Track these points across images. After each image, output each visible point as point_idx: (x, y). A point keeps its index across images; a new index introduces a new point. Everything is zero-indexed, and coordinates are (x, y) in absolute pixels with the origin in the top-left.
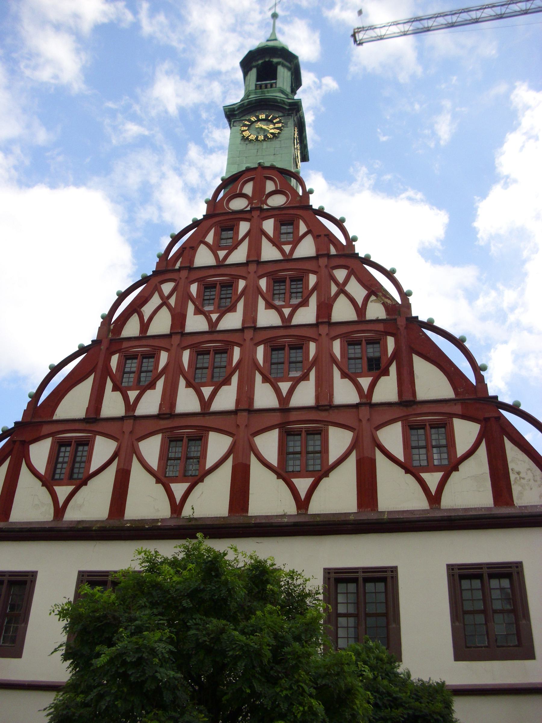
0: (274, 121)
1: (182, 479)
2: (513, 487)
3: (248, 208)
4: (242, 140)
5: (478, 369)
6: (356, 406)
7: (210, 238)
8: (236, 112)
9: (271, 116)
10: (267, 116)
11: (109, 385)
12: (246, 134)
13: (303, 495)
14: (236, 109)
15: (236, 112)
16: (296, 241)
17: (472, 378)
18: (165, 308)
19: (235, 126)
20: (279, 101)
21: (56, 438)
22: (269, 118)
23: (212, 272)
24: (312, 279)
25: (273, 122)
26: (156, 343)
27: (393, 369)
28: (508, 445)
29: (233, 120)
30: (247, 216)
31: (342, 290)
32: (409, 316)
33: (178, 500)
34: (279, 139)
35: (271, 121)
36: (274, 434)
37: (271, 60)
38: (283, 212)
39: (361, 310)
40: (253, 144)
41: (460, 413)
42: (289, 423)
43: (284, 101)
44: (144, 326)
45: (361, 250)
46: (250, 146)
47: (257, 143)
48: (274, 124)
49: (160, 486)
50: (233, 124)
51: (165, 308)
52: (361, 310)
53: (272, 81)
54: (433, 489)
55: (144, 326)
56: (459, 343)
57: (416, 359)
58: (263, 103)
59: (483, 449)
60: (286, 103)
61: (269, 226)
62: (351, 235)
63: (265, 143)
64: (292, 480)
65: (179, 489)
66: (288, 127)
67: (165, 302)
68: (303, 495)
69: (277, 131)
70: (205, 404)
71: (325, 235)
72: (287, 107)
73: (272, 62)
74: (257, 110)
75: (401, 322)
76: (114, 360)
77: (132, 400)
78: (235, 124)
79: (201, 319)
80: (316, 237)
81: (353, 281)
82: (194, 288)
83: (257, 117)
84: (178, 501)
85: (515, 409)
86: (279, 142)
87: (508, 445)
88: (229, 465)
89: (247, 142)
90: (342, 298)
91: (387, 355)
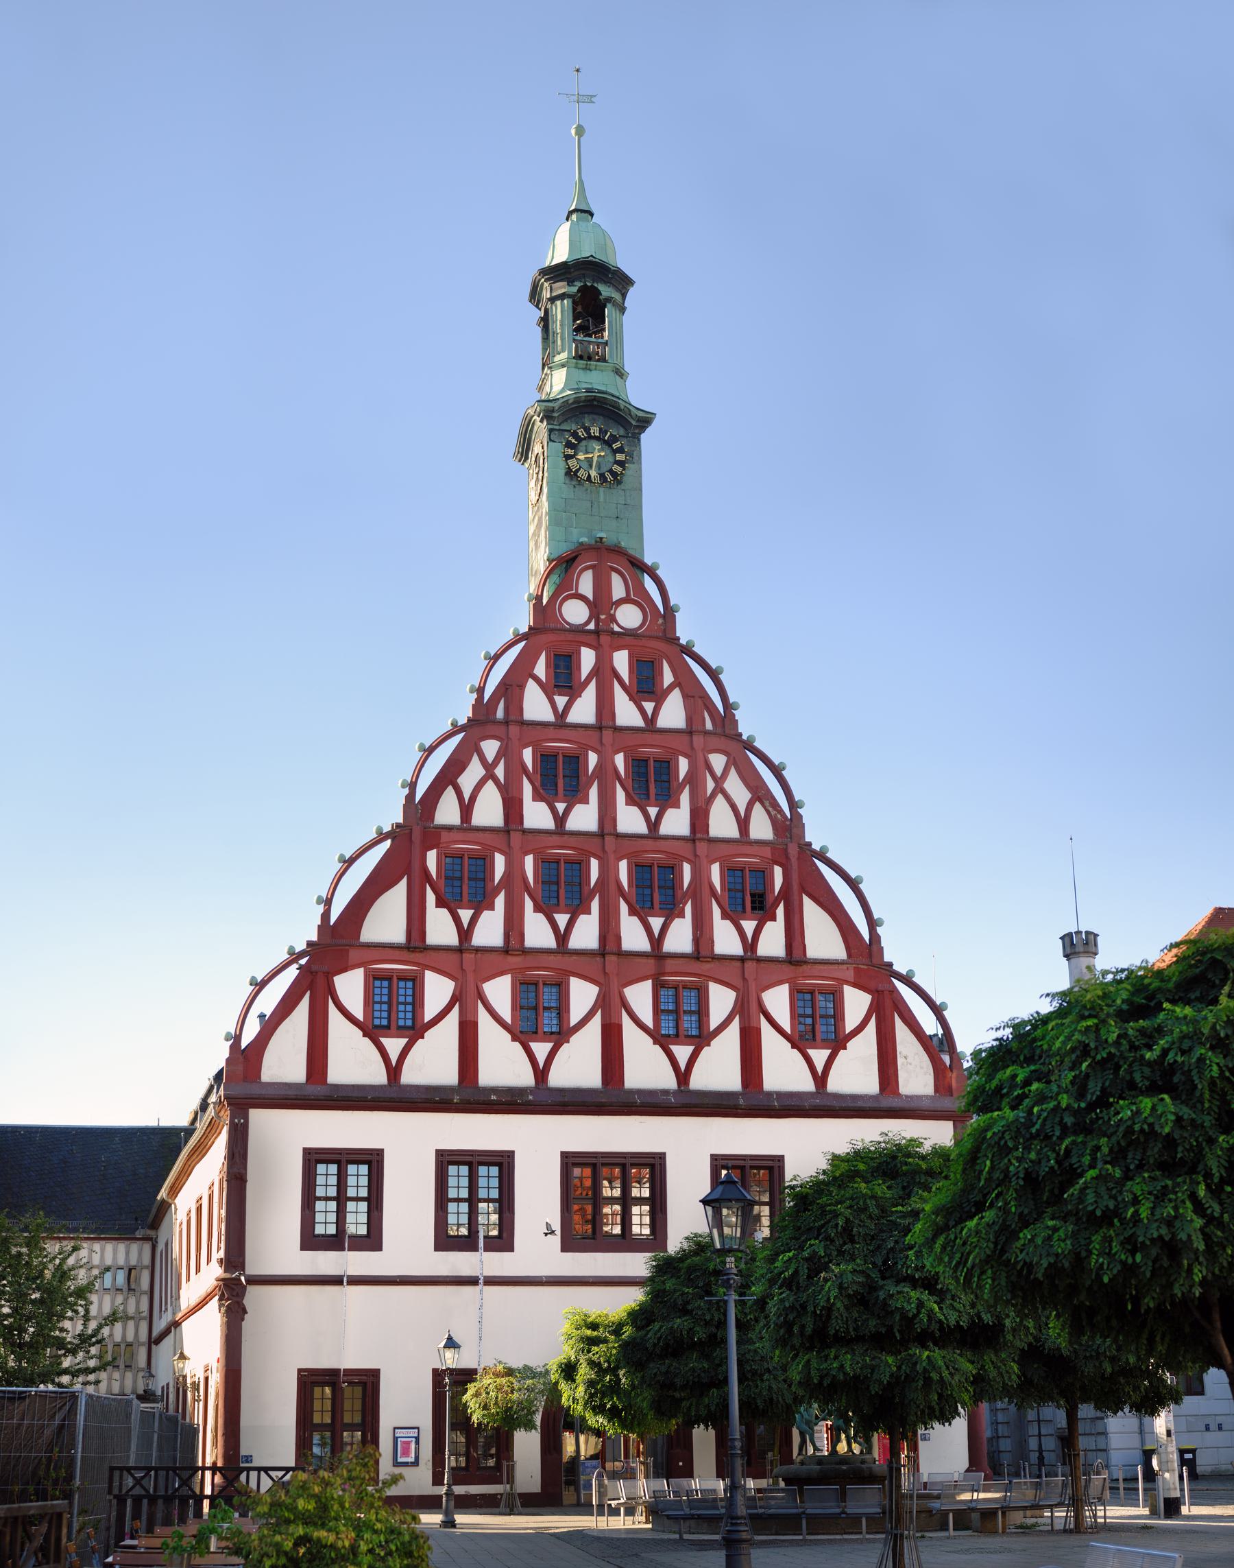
0: (615, 446)
1: (546, 1037)
2: (900, 1073)
3: (592, 626)
5: (872, 923)
6: (742, 959)
7: (540, 669)
8: (556, 415)
9: (609, 434)
11: (431, 897)
13: (683, 1066)
14: (557, 408)
15: (556, 415)
16: (659, 698)
17: (866, 934)
18: (490, 783)
19: (553, 441)
20: (622, 407)
21: (370, 969)
22: (606, 438)
23: (551, 732)
24: (683, 765)
25: (612, 448)
26: (488, 838)
27: (780, 912)
28: (899, 1023)
31: (720, 789)
32: (801, 842)
33: (541, 1064)
34: (622, 486)
35: (608, 444)
36: (647, 986)
37: (596, 285)
39: (743, 823)
40: (584, 488)
41: (853, 981)
42: (664, 974)
44: (467, 809)
45: (745, 730)
48: (615, 452)
49: (517, 1044)
51: (490, 783)
52: (743, 823)
54: (820, 1068)
55: (467, 809)
56: (853, 884)
57: (807, 901)
58: (595, 403)
59: (872, 1025)
61: (621, 660)
62: (732, 699)
63: (601, 490)
64: (671, 1047)
65: (541, 1049)
67: (490, 775)
68: (682, 1066)
70: (562, 937)
71: (701, 697)
72: (634, 423)
73: (599, 293)
74: (587, 413)
75: (793, 851)
76: (432, 858)
77: (465, 922)
79: (542, 807)
80: (686, 697)
81: (733, 776)
82: (528, 755)
83: (587, 430)
84: (541, 1064)
85: (908, 980)
87: (899, 1023)
88: (597, 1020)
89: (574, 483)
90: (720, 799)
91: (774, 892)
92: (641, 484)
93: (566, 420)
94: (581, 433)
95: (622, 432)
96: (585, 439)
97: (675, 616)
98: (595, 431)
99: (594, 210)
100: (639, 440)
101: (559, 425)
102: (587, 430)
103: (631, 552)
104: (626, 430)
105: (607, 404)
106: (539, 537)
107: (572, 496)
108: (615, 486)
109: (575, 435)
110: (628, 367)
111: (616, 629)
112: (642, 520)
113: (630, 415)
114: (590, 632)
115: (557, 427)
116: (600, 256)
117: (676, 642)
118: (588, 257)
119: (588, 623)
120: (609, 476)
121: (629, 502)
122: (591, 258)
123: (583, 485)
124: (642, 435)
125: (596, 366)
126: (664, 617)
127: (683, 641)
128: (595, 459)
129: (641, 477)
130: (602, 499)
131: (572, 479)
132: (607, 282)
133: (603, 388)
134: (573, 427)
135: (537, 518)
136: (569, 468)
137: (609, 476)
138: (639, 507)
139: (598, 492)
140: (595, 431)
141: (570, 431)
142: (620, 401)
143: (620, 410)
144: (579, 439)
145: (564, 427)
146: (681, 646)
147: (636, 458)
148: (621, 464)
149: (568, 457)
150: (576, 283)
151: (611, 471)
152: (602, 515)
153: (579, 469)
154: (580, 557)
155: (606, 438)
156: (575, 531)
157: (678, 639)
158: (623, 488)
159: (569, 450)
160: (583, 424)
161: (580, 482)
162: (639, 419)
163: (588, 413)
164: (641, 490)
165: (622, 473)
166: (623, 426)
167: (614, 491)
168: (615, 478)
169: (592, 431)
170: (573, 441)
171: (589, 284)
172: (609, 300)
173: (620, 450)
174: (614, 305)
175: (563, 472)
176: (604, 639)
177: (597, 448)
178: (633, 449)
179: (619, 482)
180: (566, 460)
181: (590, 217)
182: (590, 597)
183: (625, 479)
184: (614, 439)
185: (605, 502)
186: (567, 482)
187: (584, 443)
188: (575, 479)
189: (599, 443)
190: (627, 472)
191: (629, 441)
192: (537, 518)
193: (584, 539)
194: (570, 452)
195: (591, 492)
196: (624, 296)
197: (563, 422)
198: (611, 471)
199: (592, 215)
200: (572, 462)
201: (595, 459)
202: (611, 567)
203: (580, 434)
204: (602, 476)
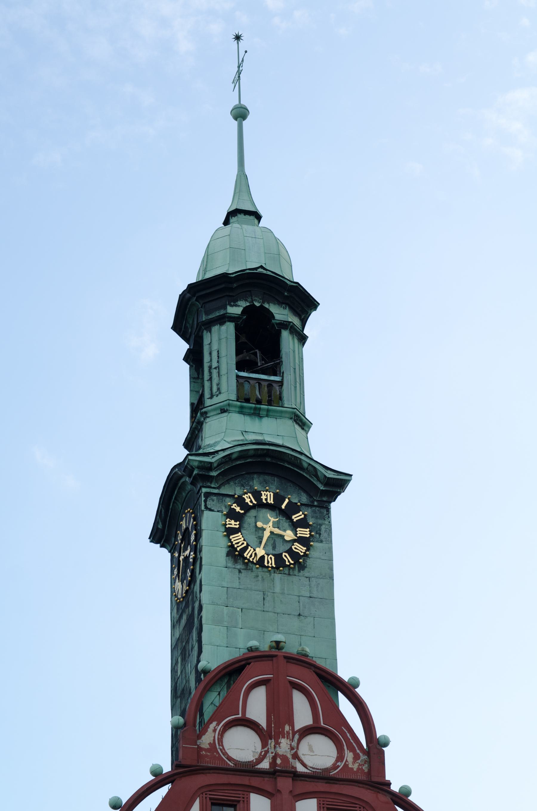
3: (265, 765)
4: (228, 554)
8: (214, 474)
9: (287, 501)
10: (279, 499)
12: (238, 539)
14: (215, 465)
15: (214, 474)
19: (210, 510)
20: (305, 465)
22: (283, 507)
29: (204, 490)
30: (266, 783)
34: (306, 573)
35: (287, 514)
37: (266, 305)
38: (335, 788)
40: (254, 574)
43: (315, 468)
46: (247, 578)
47: (260, 572)
48: (295, 526)
50: (205, 501)
53: (272, 378)
58: (268, 460)
60: (319, 474)
63: (277, 577)
66: (321, 541)
69: (299, 549)
72: (322, 488)
78: (210, 504)
83: (257, 495)
86: (306, 581)
92: (332, 569)
93: (228, 482)
94: (249, 499)
95: (304, 499)
96: (254, 507)
97: (383, 752)
98: (268, 497)
99: (261, 212)
100: (328, 510)
101: (218, 488)
102: (257, 495)
103: (320, 663)
104: (311, 497)
105: (284, 461)
106: (187, 642)
107: (236, 585)
108: (296, 572)
109: (240, 501)
110: (309, 415)
111: (300, 768)
112: (334, 619)
113: (316, 476)
114: (263, 773)
115: (216, 491)
116: (273, 267)
117: (385, 788)
118: (256, 269)
119: (260, 760)
120: (288, 559)
121: (315, 594)
122: (260, 270)
123: (251, 570)
124: (333, 505)
125: (268, 410)
126: (367, 753)
127: (395, 787)
128: (267, 534)
129: (331, 560)
130: (278, 589)
131: (236, 562)
132: (282, 302)
133: (280, 442)
134: (238, 491)
135: (185, 617)
136: (232, 546)
137: (288, 559)
138: (330, 601)
139: (273, 580)
140: (268, 497)
141: (232, 496)
142: (303, 457)
143: (302, 468)
144: (247, 508)
145: (223, 491)
146: (393, 794)
147: (324, 535)
148: (302, 541)
149: (230, 532)
150: (239, 303)
151: (290, 552)
152: (279, 611)
153: (245, 549)
154: (248, 668)
155: (283, 507)
156: (241, 633)
157: (389, 784)
158: (307, 575)
159: (233, 522)
160: (251, 487)
161: (248, 564)
162: (329, 482)
163: (259, 473)
164: (332, 578)
165: (305, 555)
166: (305, 491)
167: (295, 579)
168: (296, 562)
169: (264, 497)
170: (238, 509)
171: (257, 304)
172: (285, 325)
173: (303, 524)
174: (291, 333)
175: (224, 551)
176: (285, 784)
177: (272, 519)
178: (320, 521)
179: (302, 567)
180: (228, 536)
181: (256, 221)
182: (263, 722)
183: (309, 562)
184: (293, 508)
185: (283, 593)
186: (230, 564)
187: (253, 513)
188: (240, 561)
189: (274, 514)
190: (312, 553)
191: (314, 512)
192: (185, 617)
193: (254, 643)
194: (233, 524)
195: (263, 579)
196: (304, 323)
197: (223, 484)
198: (290, 552)
199: (258, 217)
200: (238, 539)
201: (267, 534)
202: (291, 682)
203: (248, 500)
204: (278, 558)
